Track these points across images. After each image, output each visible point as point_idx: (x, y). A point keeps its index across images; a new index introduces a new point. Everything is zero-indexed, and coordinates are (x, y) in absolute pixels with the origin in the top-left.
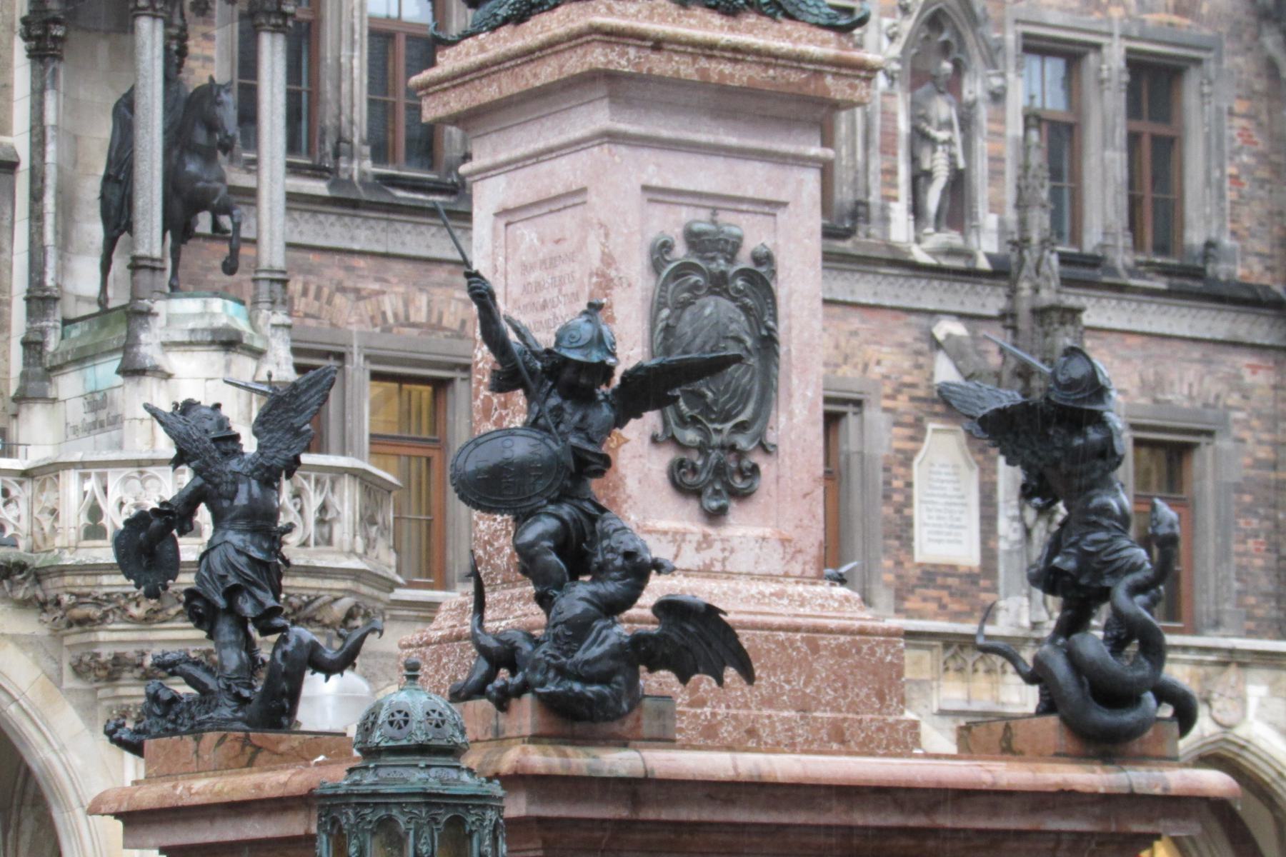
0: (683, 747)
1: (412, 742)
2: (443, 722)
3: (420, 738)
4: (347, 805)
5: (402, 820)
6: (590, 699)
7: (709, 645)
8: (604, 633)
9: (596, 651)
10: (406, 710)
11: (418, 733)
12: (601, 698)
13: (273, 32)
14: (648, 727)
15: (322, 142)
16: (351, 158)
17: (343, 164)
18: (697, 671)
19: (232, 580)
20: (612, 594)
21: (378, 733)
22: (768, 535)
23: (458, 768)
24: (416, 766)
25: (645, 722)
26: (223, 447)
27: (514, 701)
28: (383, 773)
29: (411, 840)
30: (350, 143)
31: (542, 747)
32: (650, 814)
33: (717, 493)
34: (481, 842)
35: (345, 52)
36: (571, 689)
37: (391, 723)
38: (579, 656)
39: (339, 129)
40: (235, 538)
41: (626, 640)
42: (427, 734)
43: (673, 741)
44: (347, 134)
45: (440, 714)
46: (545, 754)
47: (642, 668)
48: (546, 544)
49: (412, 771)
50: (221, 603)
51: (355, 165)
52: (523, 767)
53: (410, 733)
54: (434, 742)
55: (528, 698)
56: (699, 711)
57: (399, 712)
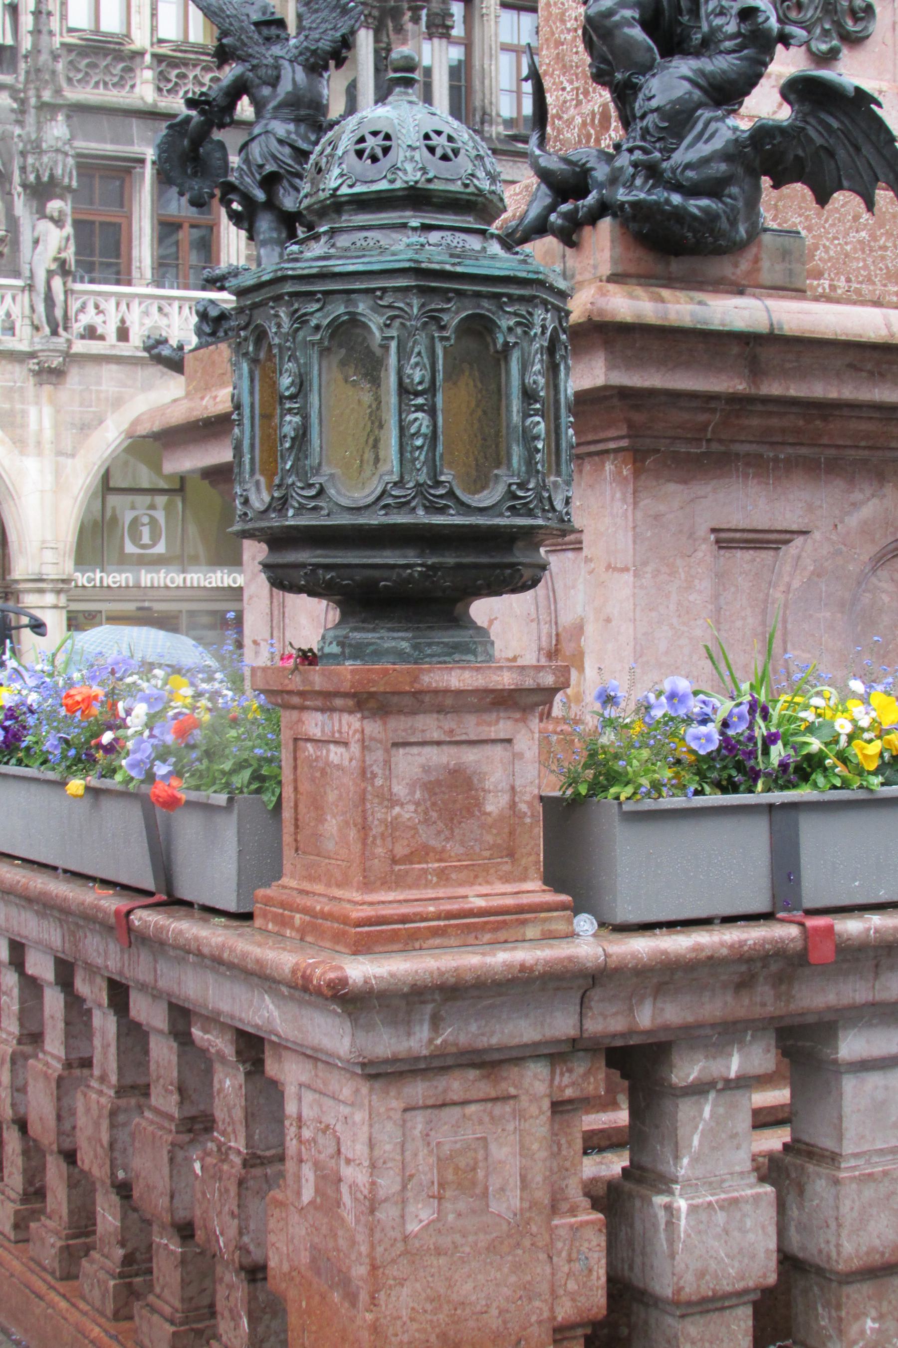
0: (817, 299)
1: (398, 185)
2: (456, 152)
3: (411, 175)
4: (278, 298)
5: (375, 322)
6: (694, 217)
7: (858, 149)
8: (713, 126)
9: (705, 149)
10: (386, 129)
11: (409, 167)
12: (711, 217)
13: (440, 38)
14: (770, 270)
15: (474, 115)
16: (491, 125)
17: (486, 128)
18: (840, 188)
19: (270, 168)
20: (724, 72)
21: (336, 171)
22: (884, 89)
23: (483, 232)
24: (404, 226)
25: (765, 264)
26: (265, 31)
27: (587, 230)
28: (343, 241)
29: (393, 360)
30: (490, 115)
31: (626, 287)
32: (774, 388)
33: (826, 33)
34: (525, 367)
35: (486, 62)
36: (668, 202)
37: (360, 154)
38: (682, 156)
39: (483, 108)
40: (281, 128)
41: (746, 135)
42: (424, 170)
43: (804, 291)
44: (488, 111)
45: (450, 139)
46: (631, 296)
47: (766, 182)
48: (628, 13)
49: (395, 236)
50: (260, 195)
51: (494, 128)
52: (601, 312)
53: (394, 168)
54: (436, 186)
55: (606, 224)
56: (815, 283)
57: (375, 134)
